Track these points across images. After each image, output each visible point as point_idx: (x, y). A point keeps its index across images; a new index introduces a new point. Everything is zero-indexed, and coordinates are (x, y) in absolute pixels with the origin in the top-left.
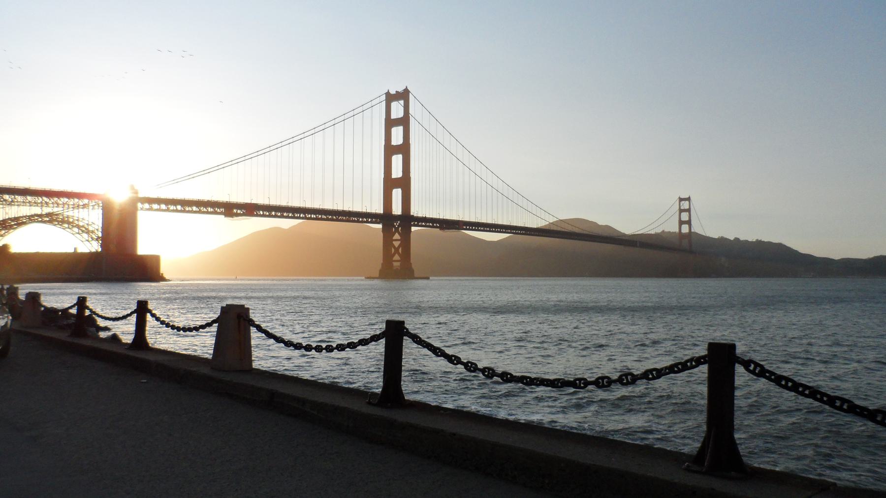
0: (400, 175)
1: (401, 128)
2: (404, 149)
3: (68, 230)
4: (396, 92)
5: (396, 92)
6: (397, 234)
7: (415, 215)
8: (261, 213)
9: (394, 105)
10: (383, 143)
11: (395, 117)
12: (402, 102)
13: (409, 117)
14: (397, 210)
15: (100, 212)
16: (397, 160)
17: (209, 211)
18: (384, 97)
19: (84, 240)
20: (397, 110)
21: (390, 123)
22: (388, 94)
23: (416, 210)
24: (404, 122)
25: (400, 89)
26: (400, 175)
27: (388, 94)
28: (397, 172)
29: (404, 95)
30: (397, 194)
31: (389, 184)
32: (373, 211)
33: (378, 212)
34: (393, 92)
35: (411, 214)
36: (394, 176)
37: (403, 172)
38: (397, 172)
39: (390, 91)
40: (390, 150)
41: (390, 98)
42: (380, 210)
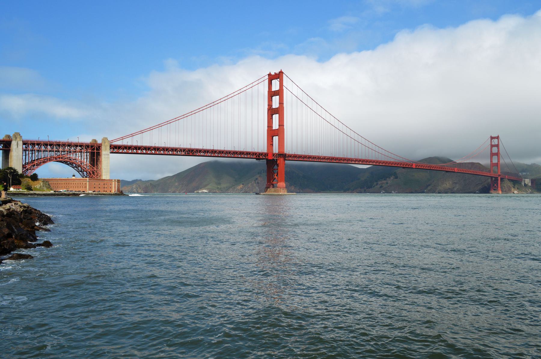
0: (277, 127)
1: (278, 97)
2: (279, 111)
3: (70, 165)
4: (275, 73)
5: (275, 73)
6: (276, 165)
7: (287, 153)
8: (209, 154)
9: (273, 81)
10: (266, 107)
11: (274, 90)
12: (278, 80)
13: (283, 90)
14: (276, 150)
15: (88, 154)
16: (276, 117)
17: (171, 153)
18: (267, 77)
19: (79, 171)
20: (276, 85)
21: (272, 94)
22: (270, 75)
23: (289, 149)
24: (279, 93)
25: (277, 72)
26: (277, 127)
27: (270, 75)
28: (276, 126)
29: (279, 76)
30: (276, 139)
31: (272, 133)
32: (260, 151)
33: (263, 151)
34: (273, 73)
35: (285, 152)
36: (274, 128)
37: (279, 125)
38: (276, 126)
39: (271, 73)
40: (272, 112)
41: (271, 78)
42: (265, 151)
